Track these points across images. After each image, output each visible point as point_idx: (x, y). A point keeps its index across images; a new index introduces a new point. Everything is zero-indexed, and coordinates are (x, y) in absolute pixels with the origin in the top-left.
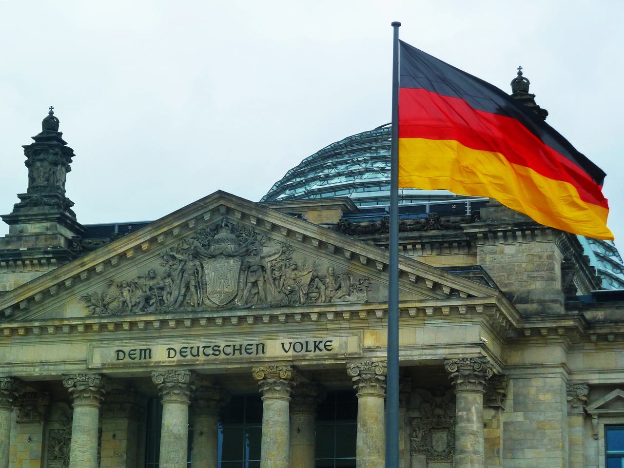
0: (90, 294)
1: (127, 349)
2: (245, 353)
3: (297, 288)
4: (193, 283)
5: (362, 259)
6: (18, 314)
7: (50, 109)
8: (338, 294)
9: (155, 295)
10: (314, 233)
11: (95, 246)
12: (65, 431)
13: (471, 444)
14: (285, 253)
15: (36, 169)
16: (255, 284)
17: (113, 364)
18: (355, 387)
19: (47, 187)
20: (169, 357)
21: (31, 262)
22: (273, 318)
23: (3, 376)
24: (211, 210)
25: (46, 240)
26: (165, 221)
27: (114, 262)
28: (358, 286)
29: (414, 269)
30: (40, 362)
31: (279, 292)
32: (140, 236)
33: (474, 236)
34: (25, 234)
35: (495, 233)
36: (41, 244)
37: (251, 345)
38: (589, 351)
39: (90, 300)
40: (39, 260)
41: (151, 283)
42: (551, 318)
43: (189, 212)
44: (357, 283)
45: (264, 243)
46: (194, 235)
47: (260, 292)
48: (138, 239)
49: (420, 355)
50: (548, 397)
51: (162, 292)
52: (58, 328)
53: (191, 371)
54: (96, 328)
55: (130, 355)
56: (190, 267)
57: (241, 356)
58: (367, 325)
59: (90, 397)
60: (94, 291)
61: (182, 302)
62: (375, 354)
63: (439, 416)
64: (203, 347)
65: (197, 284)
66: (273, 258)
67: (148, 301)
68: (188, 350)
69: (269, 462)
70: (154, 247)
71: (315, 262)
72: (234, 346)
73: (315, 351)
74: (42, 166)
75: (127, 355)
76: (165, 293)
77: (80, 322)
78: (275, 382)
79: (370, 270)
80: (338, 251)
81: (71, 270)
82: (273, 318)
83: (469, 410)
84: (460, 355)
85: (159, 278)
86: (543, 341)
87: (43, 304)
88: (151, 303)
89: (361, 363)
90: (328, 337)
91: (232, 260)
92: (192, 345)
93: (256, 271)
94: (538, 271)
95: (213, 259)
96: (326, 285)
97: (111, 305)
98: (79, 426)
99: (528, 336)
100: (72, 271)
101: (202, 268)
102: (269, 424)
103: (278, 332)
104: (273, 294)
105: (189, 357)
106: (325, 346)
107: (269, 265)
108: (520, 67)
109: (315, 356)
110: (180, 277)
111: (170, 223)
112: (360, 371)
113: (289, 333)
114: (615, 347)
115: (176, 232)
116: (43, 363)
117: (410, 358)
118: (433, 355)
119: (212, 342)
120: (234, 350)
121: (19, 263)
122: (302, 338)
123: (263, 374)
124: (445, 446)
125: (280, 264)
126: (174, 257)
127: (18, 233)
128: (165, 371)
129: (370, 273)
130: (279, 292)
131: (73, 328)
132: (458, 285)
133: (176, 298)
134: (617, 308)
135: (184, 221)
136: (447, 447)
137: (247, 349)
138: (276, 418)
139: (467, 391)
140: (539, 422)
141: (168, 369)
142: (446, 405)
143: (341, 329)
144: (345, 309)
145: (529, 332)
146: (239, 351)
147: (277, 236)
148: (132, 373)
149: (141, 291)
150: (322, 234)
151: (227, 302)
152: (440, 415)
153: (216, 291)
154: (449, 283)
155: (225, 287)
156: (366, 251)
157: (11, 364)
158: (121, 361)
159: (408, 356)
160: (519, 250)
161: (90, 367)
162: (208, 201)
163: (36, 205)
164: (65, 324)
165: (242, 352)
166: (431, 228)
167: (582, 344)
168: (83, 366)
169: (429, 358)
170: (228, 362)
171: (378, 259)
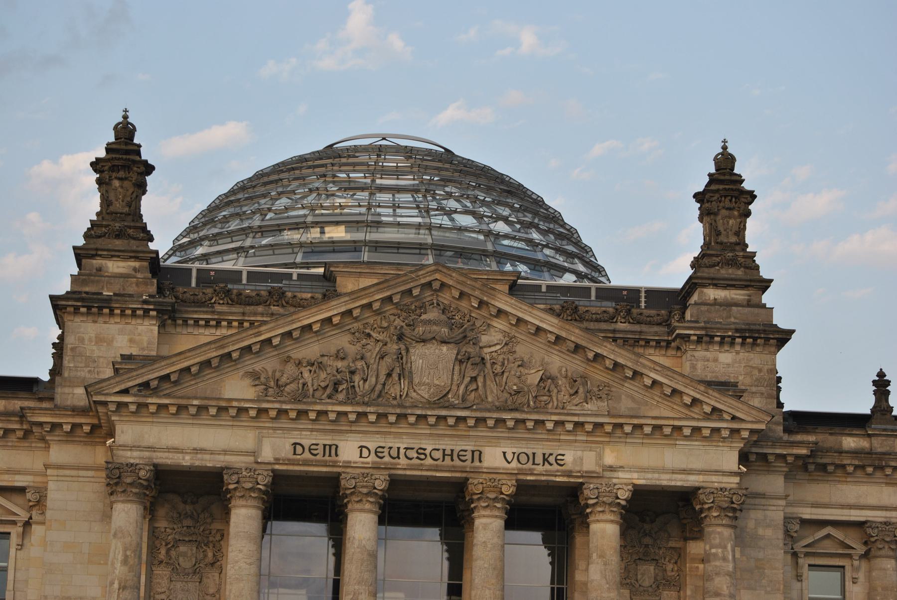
0: (257, 369)
1: (306, 443)
2: (458, 460)
3: (526, 389)
4: (397, 370)
6: (166, 386)
8: (575, 400)
9: (347, 381)
10: (552, 326)
11: (192, 297)
13: (727, 587)
16: (474, 379)
17: (289, 460)
18: (588, 510)
19: (129, 214)
20: (361, 457)
21: (123, 311)
22: (500, 422)
23: (144, 463)
25: (137, 285)
26: (367, 292)
27: (296, 334)
28: (597, 393)
29: (671, 380)
30: (193, 450)
33: (686, 338)
34: (106, 274)
35: (712, 337)
36: (131, 290)
37: (466, 451)
38: (800, 481)
39: (259, 378)
40: (134, 310)
41: (340, 364)
42: (782, 444)
43: (396, 284)
44: (595, 389)
45: (485, 330)
46: (395, 311)
47: (480, 388)
49: (669, 480)
50: (769, 533)
52: (221, 410)
53: (390, 476)
54: (273, 414)
55: (310, 450)
56: (394, 351)
61: (381, 392)
62: (615, 474)
63: (647, 546)
64: (404, 449)
66: (493, 349)
67: (337, 386)
68: (386, 450)
70: (348, 320)
71: (543, 359)
72: (444, 450)
73: (543, 465)
74: (122, 187)
75: (307, 450)
76: (357, 378)
78: (496, 498)
79: (612, 376)
80: (578, 348)
82: (500, 422)
83: (725, 547)
84: (716, 484)
85: (350, 360)
86: (765, 468)
87: (197, 376)
88: (340, 390)
89: (602, 484)
91: (445, 347)
92: (390, 445)
94: (758, 386)
95: (423, 344)
96: (558, 388)
97: (288, 387)
99: (752, 462)
100: (242, 341)
101: (407, 350)
102: (487, 547)
103: (499, 438)
104: (493, 392)
105: (387, 459)
106: (556, 460)
108: (725, 140)
109: (546, 471)
110: (377, 361)
112: (599, 493)
114: (830, 479)
115: (376, 306)
117: (658, 483)
118: (684, 481)
120: (444, 455)
121: (106, 311)
122: (527, 448)
123: (480, 486)
124: (653, 580)
125: (501, 358)
126: (369, 335)
127: (95, 271)
128: (358, 474)
129: (613, 379)
130: (502, 392)
131: (241, 411)
132: (723, 404)
134: (831, 434)
135: (388, 294)
136: (654, 582)
137: (462, 456)
139: (723, 525)
140: (757, 560)
142: (656, 533)
143: (576, 441)
145: (755, 457)
146: (450, 457)
147: (500, 324)
148: (307, 472)
149: (325, 373)
150: (561, 328)
151: (438, 398)
152: (648, 545)
154: (713, 400)
156: (614, 354)
157: (154, 448)
158: (299, 457)
159: (656, 479)
160: (736, 359)
161: (259, 461)
163: (118, 236)
164: (234, 405)
165: (454, 458)
166: (623, 320)
167: (795, 473)
168: (252, 459)
169: (679, 484)
170: (437, 469)
171: (629, 364)
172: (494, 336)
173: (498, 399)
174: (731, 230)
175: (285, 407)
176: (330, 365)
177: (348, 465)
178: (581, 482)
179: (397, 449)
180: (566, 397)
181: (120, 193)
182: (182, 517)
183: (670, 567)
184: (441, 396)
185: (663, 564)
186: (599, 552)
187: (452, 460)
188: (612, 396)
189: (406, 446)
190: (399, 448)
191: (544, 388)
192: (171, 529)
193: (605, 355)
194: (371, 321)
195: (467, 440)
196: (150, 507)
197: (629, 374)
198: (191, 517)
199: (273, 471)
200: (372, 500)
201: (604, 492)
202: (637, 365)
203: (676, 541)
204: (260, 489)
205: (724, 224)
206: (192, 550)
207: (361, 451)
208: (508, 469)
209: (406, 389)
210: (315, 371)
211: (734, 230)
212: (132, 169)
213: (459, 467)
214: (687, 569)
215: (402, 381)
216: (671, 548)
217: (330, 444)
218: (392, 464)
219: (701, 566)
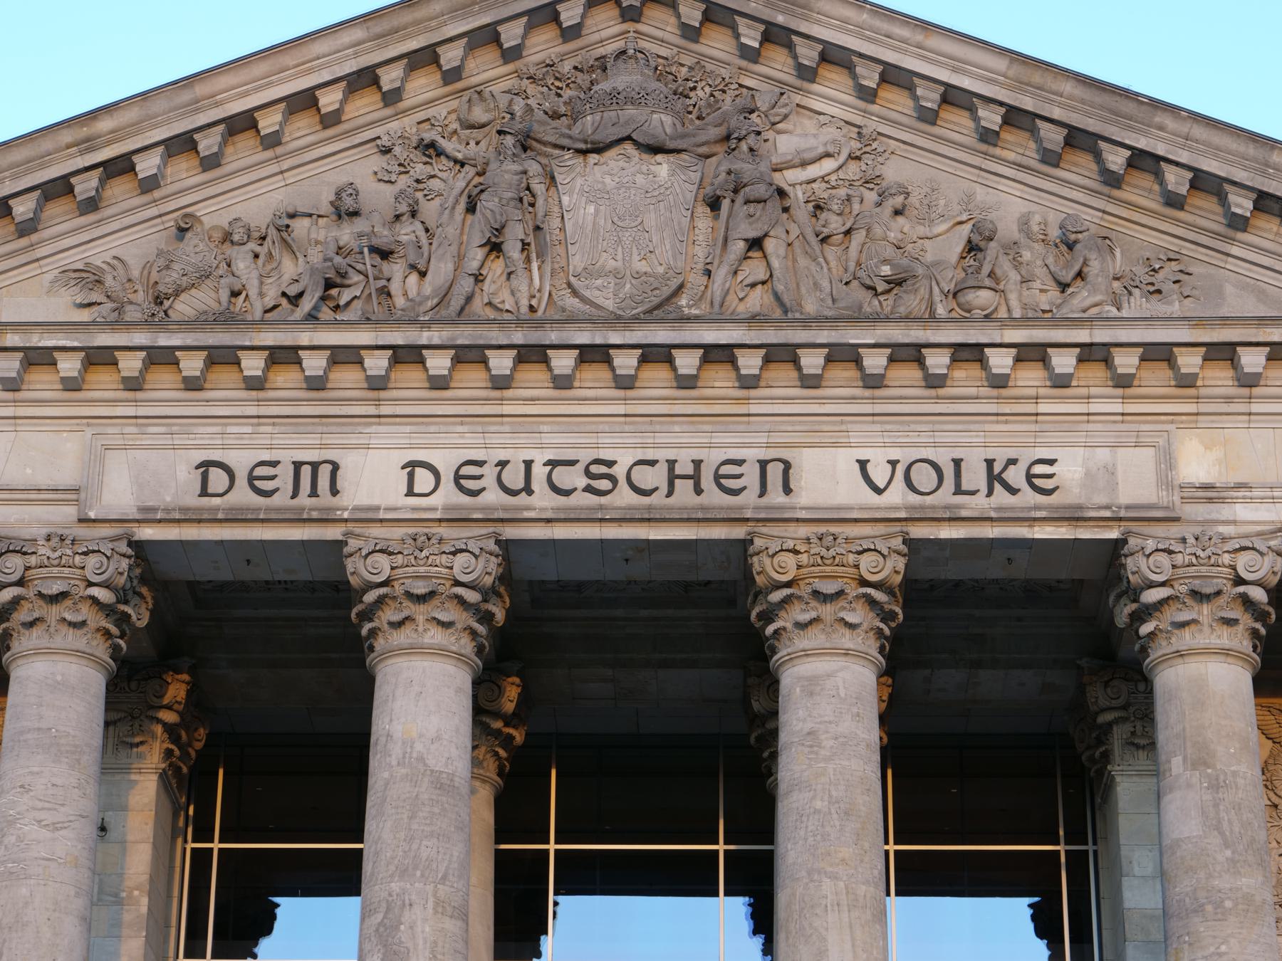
0: (99, 263)
1: (241, 461)
3: (920, 271)
9: (367, 277)
14: (858, 158)
16: (756, 244)
18: (1145, 629)
20: (410, 493)
31: (847, 283)
37: (740, 463)
41: (346, 234)
44: (1140, 271)
47: (777, 273)
48: (310, 71)
55: (251, 479)
57: (698, 500)
58: (1191, 408)
60: (114, 252)
61: (469, 299)
62: (1225, 512)
64: (544, 465)
66: (813, 171)
67: (334, 292)
68: (490, 472)
69: (827, 885)
70: (365, 105)
71: (970, 197)
72: (672, 463)
73: (990, 493)
75: (242, 481)
76: (396, 269)
77: (76, 339)
81: (42, 161)
85: (376, 218)
91: (665, 166)
92: (502, 455)
93: (765, 201)
97: (183, 297)
98: (39, 729)
100: (42, 167)
105: (493, 496)
106: (1030, 477)
109: (995, 509)
111: (433, 23)
113: (888, 427)
120: (672, 478)
133: (447, 284)
135: (486, 19)
138: (847, 726)
141: (411, 531)
144: (1124, 335)
146: (691, 482)
149: (301, 259)
151: (646, 306)
153: (604, 266)
155: (636, 257)
158: (216, 501)
161: (92, 515)
165: (704, 485)
168: (68, 512)
171: (1240, 175)
172: (815, 136)
173: (834, 301)
175: (164, 340)
176: (317, 242)
177: (370, 515)
178: (1116, 540)
179: (522, 466)
184: (656, 301)
186: (1189, 751)
187: (698, 491)
190: (528, 464)
193: (1160, 150)
194: (440, 111)
195: (742, 428)
199: (140, 549)
202: (1264, 174)
204: (94, 600)
207: (411, 476)
208: (878, 508)
209: (547, 288)
215: (535, 266)
217: (315, 459)
218: (505, 509)
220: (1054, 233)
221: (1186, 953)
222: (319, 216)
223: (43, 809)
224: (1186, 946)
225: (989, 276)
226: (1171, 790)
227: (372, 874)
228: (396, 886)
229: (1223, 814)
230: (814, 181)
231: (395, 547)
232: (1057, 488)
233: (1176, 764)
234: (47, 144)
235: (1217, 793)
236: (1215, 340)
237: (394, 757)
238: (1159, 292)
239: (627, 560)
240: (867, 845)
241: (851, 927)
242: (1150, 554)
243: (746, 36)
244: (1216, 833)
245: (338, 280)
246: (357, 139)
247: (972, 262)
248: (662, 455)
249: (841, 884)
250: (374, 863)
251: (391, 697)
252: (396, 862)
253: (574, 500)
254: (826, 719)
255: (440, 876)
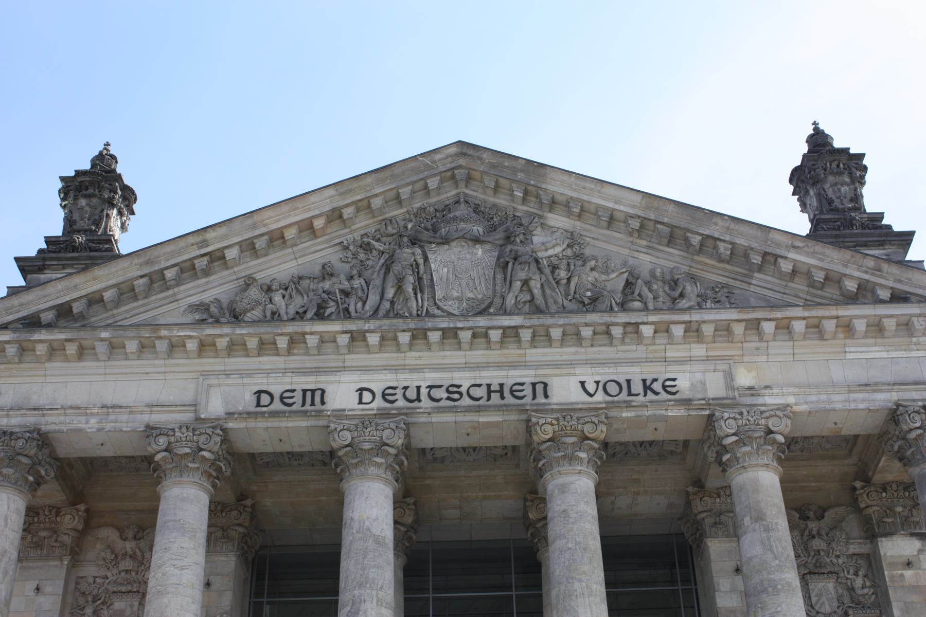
0: (207, 301)
1: (276, 390)
3: (605, 293)
5: (722, 246)
7: (105, 145)
12: (107, 578)
15: (78, 209)
16: (526, 283)
20: (360, 402)
24: (441, 172)
30: (103, 407)
31: (570, 300)
32: (313, 204)
37: (522, 384)
39: (208, 309)
41: (327, 285)
44: (709, 293)
48: (309, 210)
49: (846, 401)
51: (347, 299)
54: (222, 343)
55: (282, 398)
58: (740, 352)
59: (198, 468)
60: (214, 297)
61: (388, 312)
64: (426, 388)
65: (417, 283)
67: (322, 311)
68: (399, 392)
72: (489, 386)
73: (645, 395)
76: (352, 301)
77: (195, 332)
81: (180, 252)
85: (342, 277)
87: (115, 311)
90: (670, 372)
92: (406, 384)
95: (446, 247)
97: (249, 314)
98: (175, 520)
101: (426, 259)
105: (401, 403)
106: (664, 387)
107: (545, 262)
110: (382, 276)
116: (108, 408)
119: (444, 378)
120: (489, 392)
124: (836, 604)
133: (377, 306)
136: (839, 607)
142: (827, 535)
143: (690, 360)
146: (498, 394)
149: (305, 297)
152: (819, 551)
158: (264, 409)
161: (203, 416)
162: (437, 157)
171: (755, 245)
174: (845, 197)
179: (415, 389)
180: (667, 304)
181: (87, 211)
182: (119, 558)
183: (859, 582)
185: (847, 579)
186: (753, 514)
187: (503, 398)
188: (736, 300)
189: (428, 384)
190: (418, 388)
191: (633, 293)
192: (103, 578)
196: (72, 548)
197: (757, 259)
198: (131, 557)
200: (379, 460)
201: (746, 425)
203: (860, 543)
205: (834, 192)
206: (132, 606)
210: (291, 297)
211: (848, 198)
212: (103, 187)
213: (514, 405)
214: (887, 579)
215: (419, 296)
216: (854, 554)
218: (408, 408)
219: (908, 573)
220: (668, 277)
221: (760, 613)
222: (314, 278)
223: (176, 559)
224: (759, 609)
225: (638, 295)
226: (745, 533)
227: (345, 588)
228: (356, 592)
229: (773, 543)
230: (552, 257)
231: (353, 428)
232: (677, 392)
233: (747, 521)
234: (182, 243)
235: (769, 532)
236: (750, 317)
237: (354, 529)
238: (719, 302)
239: (468, 434)
240: (595, 565)
241: (590, 605)
242: (726, 420)
243: (516, 191)
244: (770, 552)
245: (324, 305)
246: (332, 243)
247: (629, 290)
248: (484, 382)
249: (584, 584)
250: (345, 582)
251: (352, 501)
252: (357, 580)
253: (441, 404)
254: (572, 504)
255: (379, 587)
